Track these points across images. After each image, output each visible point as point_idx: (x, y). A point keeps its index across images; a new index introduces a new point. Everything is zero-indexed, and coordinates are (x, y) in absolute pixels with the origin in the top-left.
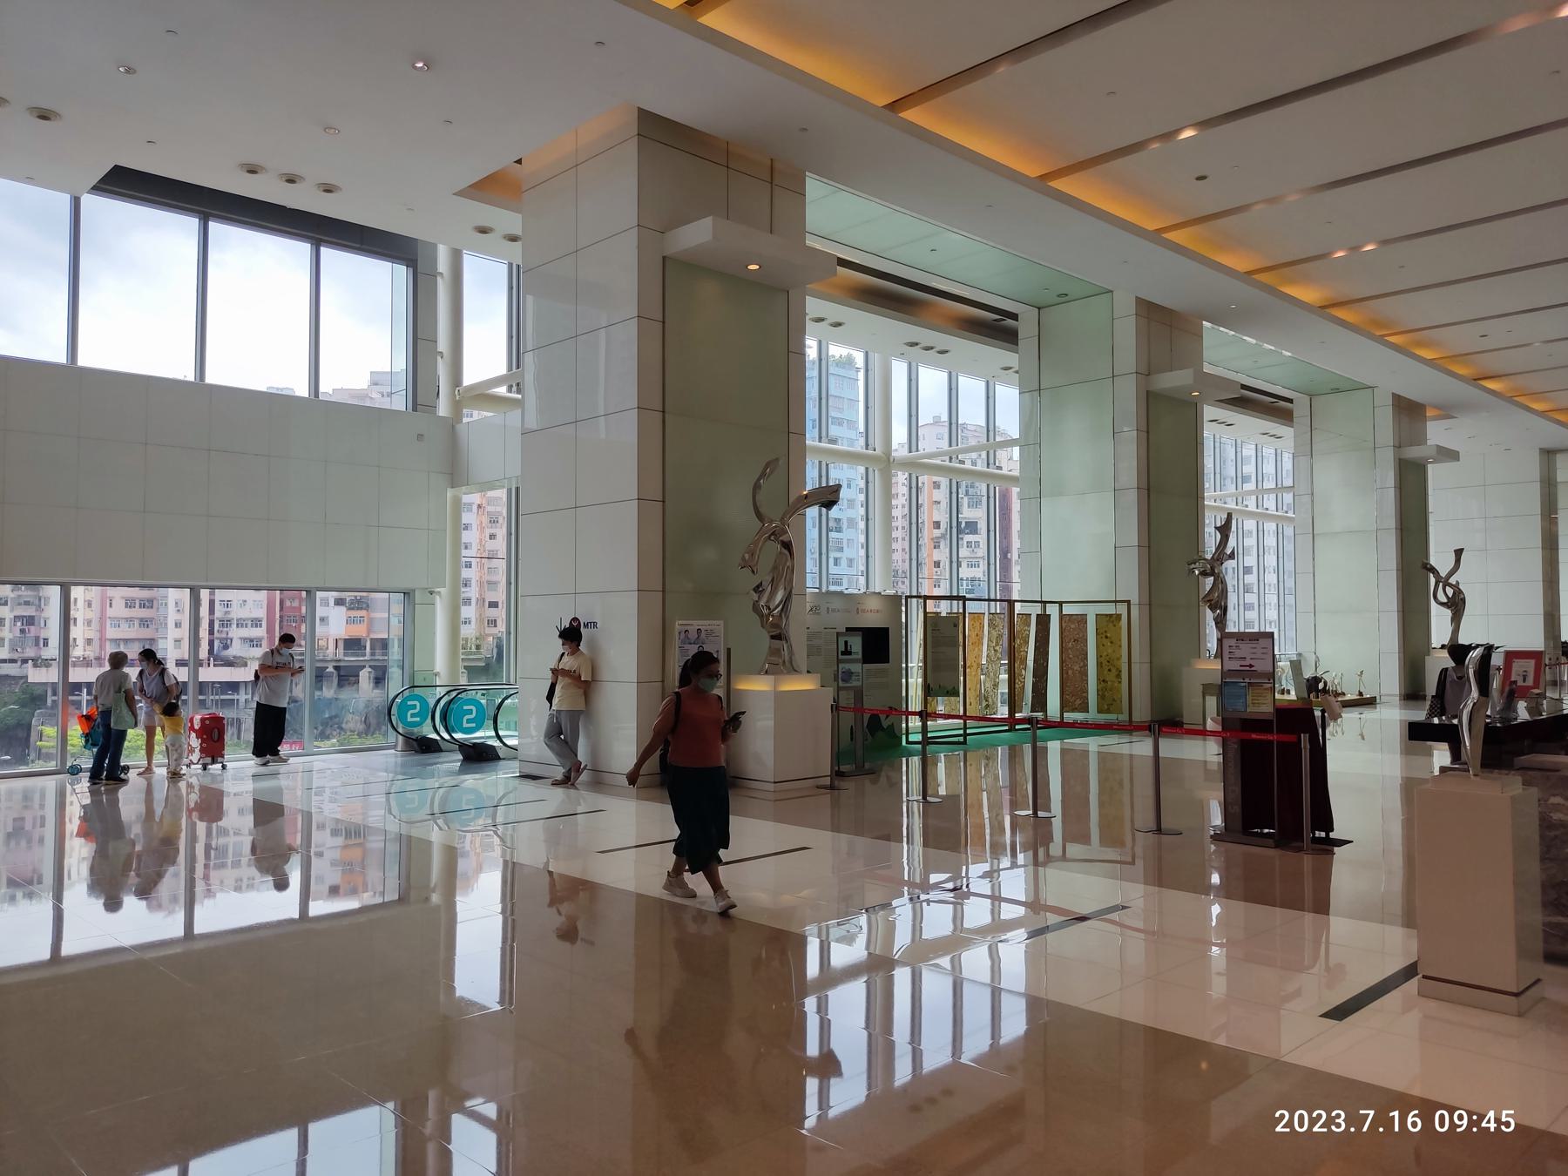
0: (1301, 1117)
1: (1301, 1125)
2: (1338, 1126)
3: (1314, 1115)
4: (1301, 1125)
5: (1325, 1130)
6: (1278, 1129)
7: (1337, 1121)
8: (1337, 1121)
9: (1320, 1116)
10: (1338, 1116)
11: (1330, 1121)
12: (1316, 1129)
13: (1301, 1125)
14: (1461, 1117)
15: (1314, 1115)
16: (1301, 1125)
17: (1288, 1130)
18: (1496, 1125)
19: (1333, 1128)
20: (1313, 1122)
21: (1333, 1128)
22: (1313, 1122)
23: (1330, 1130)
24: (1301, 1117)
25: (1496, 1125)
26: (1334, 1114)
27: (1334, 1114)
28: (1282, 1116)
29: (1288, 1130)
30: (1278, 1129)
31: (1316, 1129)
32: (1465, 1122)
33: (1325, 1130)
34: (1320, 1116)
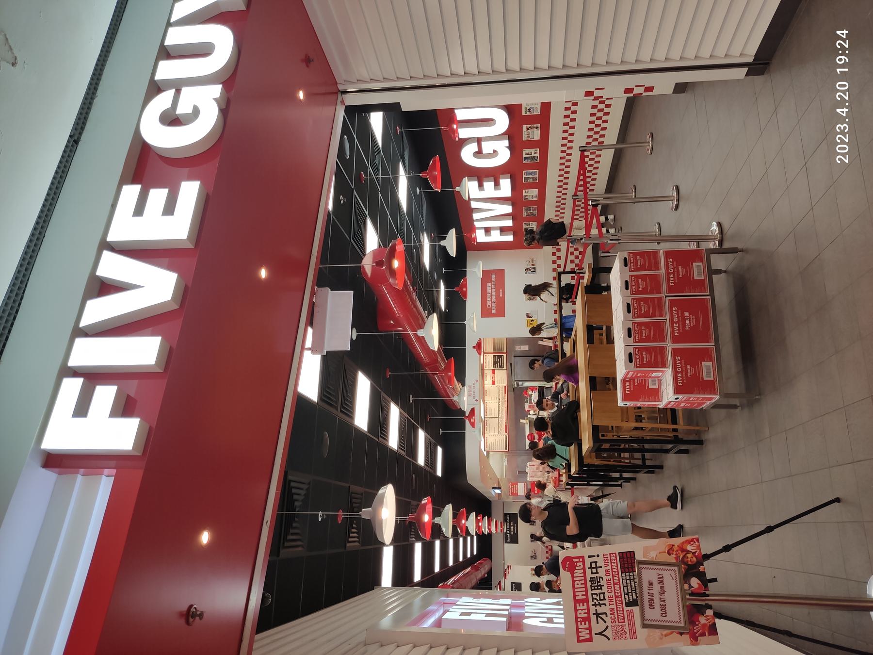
0: (840, 149)
1: (845, 149)
2: (845, 128)
3: (839, 141)
4: (845, 149)
5: (847, 135)
6: (847, 161)
7: (842, 129)
8: (842, 129)
9: (840, 138)
10: (840, 128)
11: (842, 132)
12: (847, 141)
13: (845, 149)
14: (840, 60)
15: (839, 141)
16: (845, 149)
17: (847, 156)
18: (845, 30)
19: (846, 131)
20: (843, 142)
21: (846, 131)
22: (843, 142)
23: (847, 133)
24: (840, 149)
25: (845, 30)
26: (838, 131)
27: (838, 131)
28: (840, 159)
29: (847, 156)
30: (847, 161)
31: (847, 141)
32: (843, 57)
33: (847, 135)
34: (840, 138)
